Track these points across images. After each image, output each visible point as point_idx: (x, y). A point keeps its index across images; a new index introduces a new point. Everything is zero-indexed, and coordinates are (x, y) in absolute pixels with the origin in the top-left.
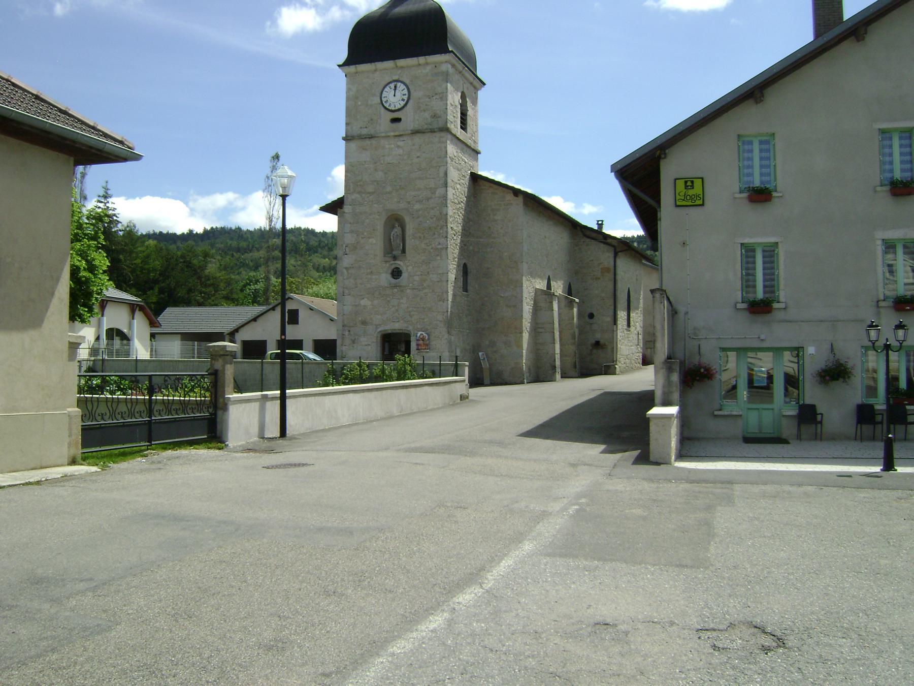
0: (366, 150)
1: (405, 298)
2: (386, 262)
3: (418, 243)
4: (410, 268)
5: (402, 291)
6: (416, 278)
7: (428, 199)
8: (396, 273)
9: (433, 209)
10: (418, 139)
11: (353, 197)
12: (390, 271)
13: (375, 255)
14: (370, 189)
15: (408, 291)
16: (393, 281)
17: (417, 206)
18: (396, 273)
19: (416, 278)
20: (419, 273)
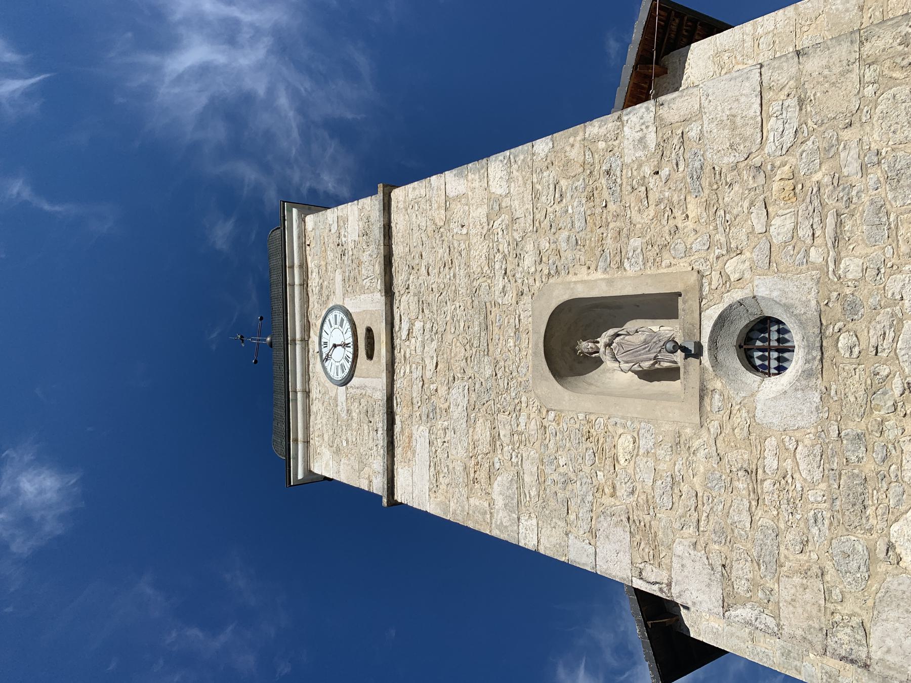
0: (410, 437)
1: (894, 285)
2: (703, 393)
3: (636, 242)
4: (733, 266)
5: (852, 308)
6: (781, 227)
7: (514, 220)
8: (759, 341)
9: (536, 196)
10: (399, 280)
11: (500, 502)
12: (752, 378)
13: (678, 443)
14: (482, 432)
15: (851, 266)
16: (797, 363)
17: (528, 261)
18: (759, 341)
19: (781, 227)
20: (757, 221)
